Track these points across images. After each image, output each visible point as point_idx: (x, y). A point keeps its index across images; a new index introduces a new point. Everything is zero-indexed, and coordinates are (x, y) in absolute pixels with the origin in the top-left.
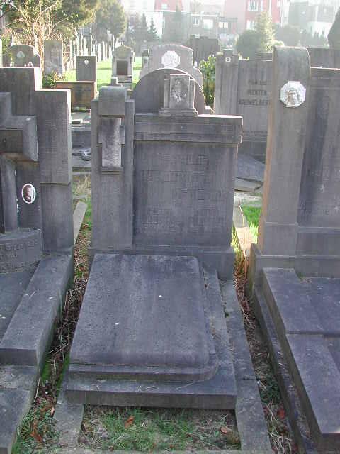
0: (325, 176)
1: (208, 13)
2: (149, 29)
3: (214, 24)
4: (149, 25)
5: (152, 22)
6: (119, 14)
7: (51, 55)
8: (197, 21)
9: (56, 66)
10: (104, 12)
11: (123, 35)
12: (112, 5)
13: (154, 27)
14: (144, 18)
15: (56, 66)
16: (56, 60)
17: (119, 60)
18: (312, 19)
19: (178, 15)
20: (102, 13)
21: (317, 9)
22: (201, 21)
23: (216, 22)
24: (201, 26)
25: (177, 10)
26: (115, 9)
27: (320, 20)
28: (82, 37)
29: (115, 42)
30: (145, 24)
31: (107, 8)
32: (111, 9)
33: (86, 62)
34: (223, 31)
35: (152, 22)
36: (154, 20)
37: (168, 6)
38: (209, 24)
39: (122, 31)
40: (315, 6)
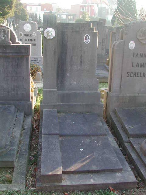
0: (69, 68)
1: (64, 12)
2: (38, 19)
3: (66, 17)
4: (38, 17)
5: (40, 16)
6: (25, 13)
10: (19, 12)
13: (40, 18)
14: (36, 14)
18: (108, 14)
20: (18, 13)
23: (67, 16)
24: (61, 17)
25: (50, 11)
28: (7, 22)
30: (36, 17)
31: (20, 10)
32: (21, 11)
35: (40, 16)
38: (64, 17)
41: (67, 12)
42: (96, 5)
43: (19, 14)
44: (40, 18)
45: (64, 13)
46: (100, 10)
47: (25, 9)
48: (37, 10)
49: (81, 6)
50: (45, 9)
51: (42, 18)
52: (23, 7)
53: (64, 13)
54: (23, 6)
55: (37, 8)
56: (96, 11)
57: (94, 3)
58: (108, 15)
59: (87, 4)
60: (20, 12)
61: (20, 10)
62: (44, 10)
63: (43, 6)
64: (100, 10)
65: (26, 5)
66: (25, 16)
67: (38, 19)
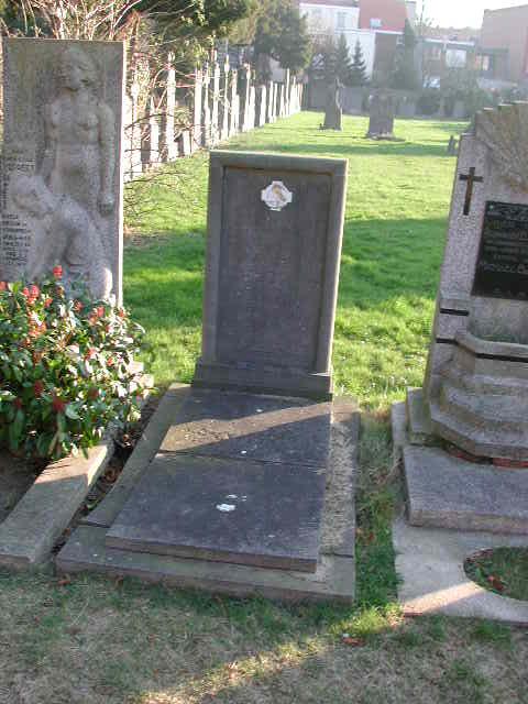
1: (455, 39)
2: (352, 62)
4: (351, 53)
5: (358, 49)
6: (302, 32)
7: (46, 141)
9: (72, 212)
10: (271, 24)
12: (285, 12)
13: (361, 60)
15: (72, 212)
16: (75, 174)
17: (504, 197)
19: (410, 38)
20: (266, 27)
22: (444, 53)
23: (472, 54)
26: (292, 21)
28: (227, 67)
29: (291, 83)
30: (343, 51)
31: (276, 16)
33: (276, 196)
34: (482, 73)
35: (358, 49)
37: (382, 23)
39: (301, 62)
41: (471, 39)
44: (357, 57)
45: (453, 42)
47: (301, 16)
50: (376, 22)
51: (368, 58)
53: (453, 42)
60: (277, 23)
61: (276, 16)
66: (300, 43)
67: (348, 61)
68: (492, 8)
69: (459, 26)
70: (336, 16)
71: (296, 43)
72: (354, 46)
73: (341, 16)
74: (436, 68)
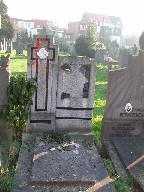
1: (60, 30)
2: (29, 36)
4: (29, 34)
5: (31, 33)
6: (12, 28)
8: (55, 34)
11: (14, 39)
14: (26, 30)
18: (111, 34)
21: (113, 29)
23: (64, 35)
27: (114, 35)
30: (27, 33)
35: (31, 33)
36: (31, 32)
38: (61, 35)
39: (13, 36)
40: (112, 28)
41: (64, 31)
42: (98, 24)
43: (4, 29)
44: (31, 35)
45: (60, 31)
46: (103, 29)
48: (29, 27)
49: (80, 24)
50: (39, 26)
52: (11, 21)
53: (60, 31)
54: (9, 19)
55: (29, 25)
56: (98, 31)
57: (96, 22)
58: (112, 35)
59: (88, 22)
62: (37, 27)
63: (36, 23)
64: (103, 29)
65: (18, 20)
67: (28, 36)
68: (71, 22)
69: (63, 27)
70: (28, 24)
71: (11, 31)
72: (30, 32)
73: (29, 25)
74: (57, 37)
